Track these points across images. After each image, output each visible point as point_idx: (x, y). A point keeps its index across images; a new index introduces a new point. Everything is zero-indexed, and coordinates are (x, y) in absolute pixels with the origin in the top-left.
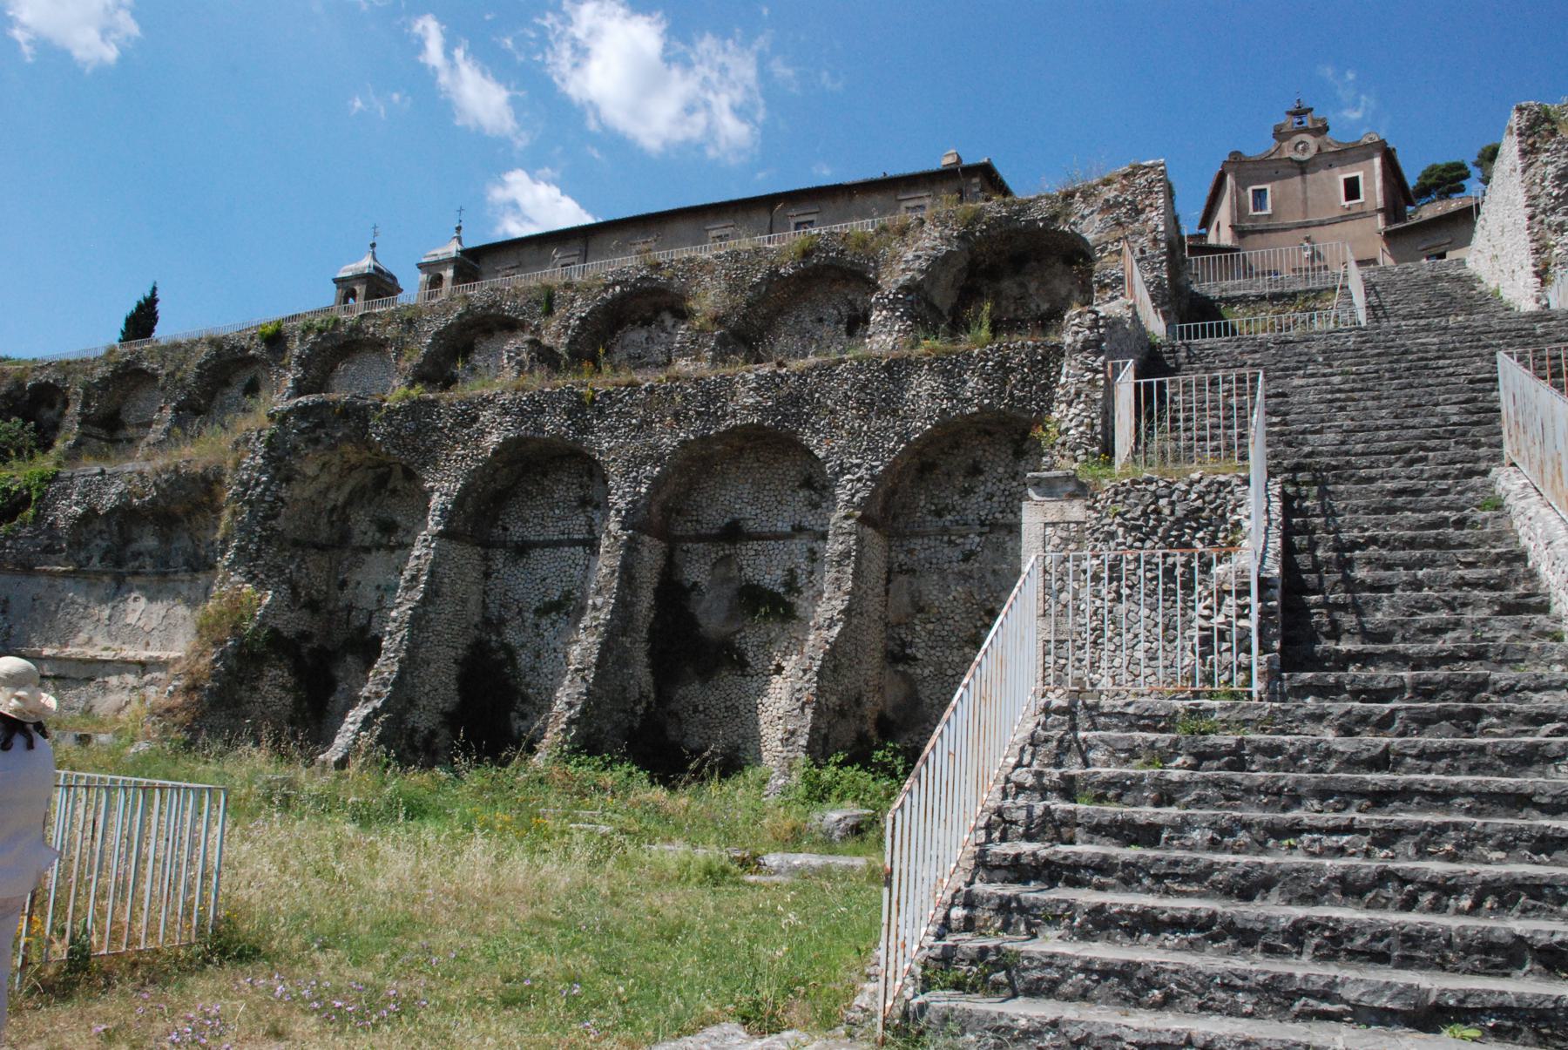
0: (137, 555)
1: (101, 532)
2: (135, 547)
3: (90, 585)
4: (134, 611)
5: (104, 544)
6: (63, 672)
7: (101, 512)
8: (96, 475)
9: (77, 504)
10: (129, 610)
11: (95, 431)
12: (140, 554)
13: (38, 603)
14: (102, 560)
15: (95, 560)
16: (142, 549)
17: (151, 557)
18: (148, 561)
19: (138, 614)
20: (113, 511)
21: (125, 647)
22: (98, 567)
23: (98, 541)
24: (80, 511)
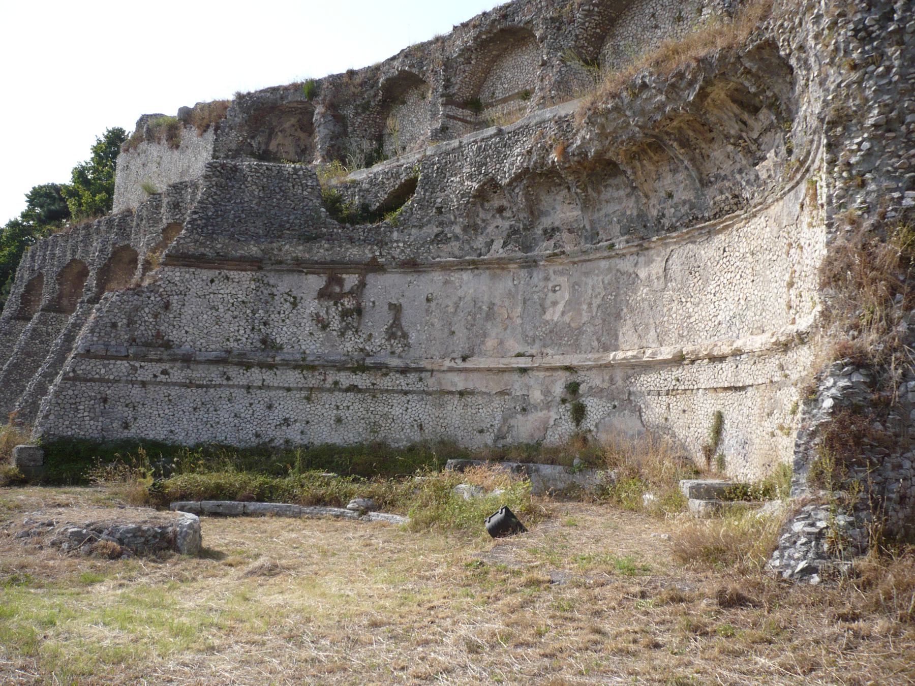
0: (550, 233)
1: (501, 210)
2: (546, 222)
3: (493, 277)
4: (555, 303)
5: (507, 224)
6: (471, 386)
7: (505, 182)
8: (491, 137)
9: (470, 177)
10: (548, 303)
11: (460, 112)
12: (555, 230)
13: (433, 304)
14: (505, 244)
15: (497, 245)
16: (556, 224)
17: (570, 231)
18: (565, 235)
19: (560, 307)
20: (518, 178)
21: (549, 351)
22: (502, 253)
23: (499, 221)
24: (476, 185)
